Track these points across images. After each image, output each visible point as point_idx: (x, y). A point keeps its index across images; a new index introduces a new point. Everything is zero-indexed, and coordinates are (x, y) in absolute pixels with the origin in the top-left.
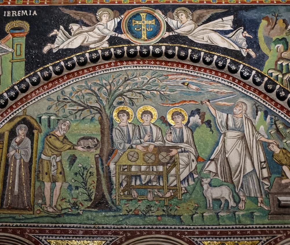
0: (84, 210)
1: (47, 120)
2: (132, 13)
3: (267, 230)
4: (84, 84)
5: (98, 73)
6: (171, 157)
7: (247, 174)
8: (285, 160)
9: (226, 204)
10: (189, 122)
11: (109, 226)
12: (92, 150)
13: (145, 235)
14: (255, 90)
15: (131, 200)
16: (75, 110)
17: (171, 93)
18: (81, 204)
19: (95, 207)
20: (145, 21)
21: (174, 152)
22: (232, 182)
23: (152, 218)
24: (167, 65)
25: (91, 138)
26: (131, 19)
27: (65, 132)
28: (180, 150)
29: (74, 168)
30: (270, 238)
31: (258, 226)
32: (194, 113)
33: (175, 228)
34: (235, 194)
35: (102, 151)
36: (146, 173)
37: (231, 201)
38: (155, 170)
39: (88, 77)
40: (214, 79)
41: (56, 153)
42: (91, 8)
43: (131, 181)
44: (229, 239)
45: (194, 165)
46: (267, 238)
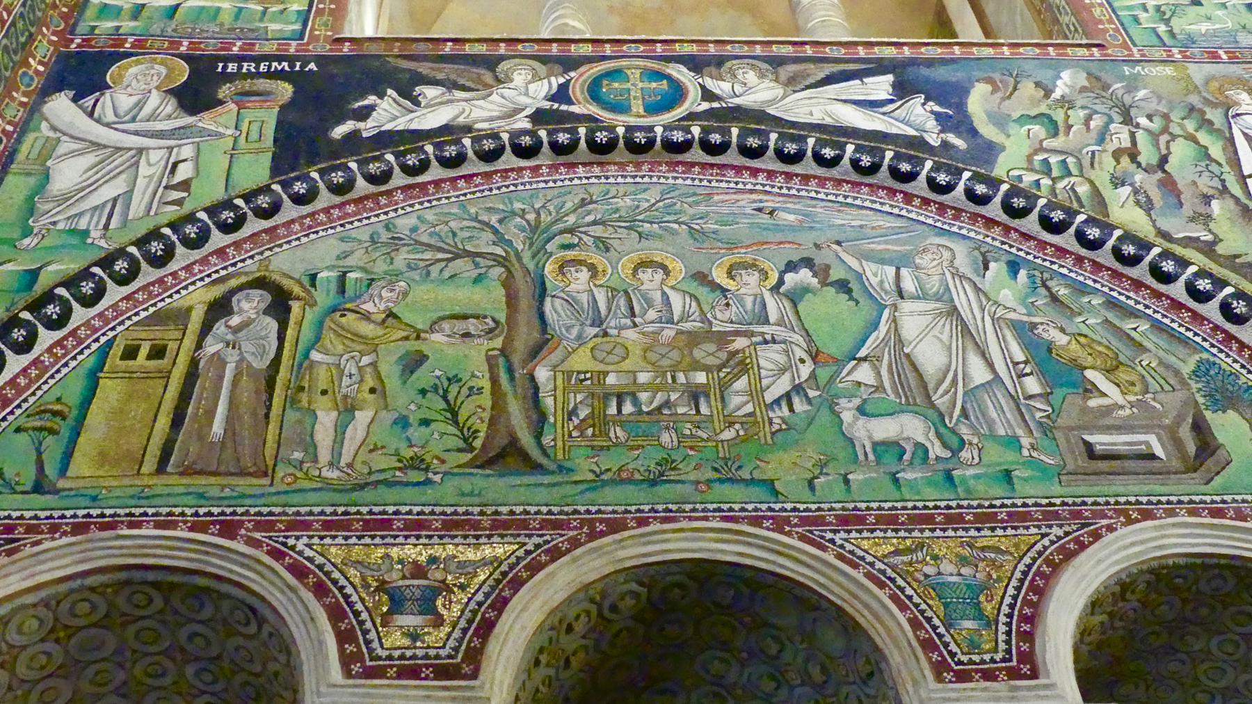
0: (445, 474)
2: (595, 69)
3: (1064, 511)
4: (455, 210)
6: (733, 354)
7: (977, 387)
9: (920, 453)
10: (781, 282)
14: (974, 217)
15: (608, 448)
16: (427, 260)
18: (438, 458)
19: (489, 463)
22: (932, 405)
25: (477, 317)
30: (1075, 527)
32: (796, 266)
34: (942, 430)
35: (509, 340)
36: (654, 389)
37: (933, 445)
38: (681, 378)
43: (606, 406)
45: (805, 370)
46: (1067, 529)
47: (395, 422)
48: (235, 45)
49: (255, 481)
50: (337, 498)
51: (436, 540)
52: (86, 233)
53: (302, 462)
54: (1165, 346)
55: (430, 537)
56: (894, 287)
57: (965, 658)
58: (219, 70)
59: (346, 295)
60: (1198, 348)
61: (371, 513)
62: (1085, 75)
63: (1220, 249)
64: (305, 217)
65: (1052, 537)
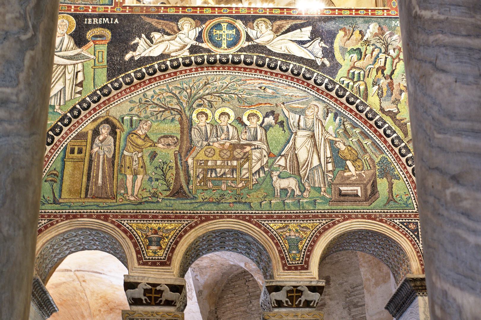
0: (163, 199)
1: (129, 121)
4: (165, 88)
5: (179, 77)
8: (350, 156)
10: (263, 122)
11: (185, 212)
12: (172, 147)
13: (218, 219)
14: (327, 95)
16: (157, 111)
17: (248, 96)
18: (161, 193)
20: (226, 31)
21: (248, 149)
23: (225, 205)
24: (246, 71)
25: (171, 137)
26: (212, 28)
27: (146, 131)
28: (253, 147)
29: (154, 163)
30: (329, 220)
31: (319, 211)
33: (245, 213)
34: (301, 185)
35: (180, 148)
36: (221, 167)
38: (230, 164)
39: (170, 81)
40: (290, 84)
41: (138, 150)
42: (173, 17)
43: (207, 174)
44: (292, 222)
45: (265, 160)
46: (327, 221)
47: (148, 180)
48: (89, 8)
49: (112, 201)
50: (134, 207)
51: (160, 222)
52: (54, 106)
53: (124, 194)
54: (374, 151)
55: (159, 221)
56: (297, 125)
57: (291, 263)
58: (86, 23)
59: (133, 127)
60: (382, 152)
61: (143, 212)
62: (378, 26)
63: (398, 117)
64: (119, 93)
65: (322, 224)
